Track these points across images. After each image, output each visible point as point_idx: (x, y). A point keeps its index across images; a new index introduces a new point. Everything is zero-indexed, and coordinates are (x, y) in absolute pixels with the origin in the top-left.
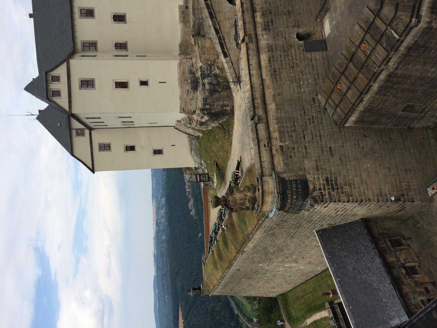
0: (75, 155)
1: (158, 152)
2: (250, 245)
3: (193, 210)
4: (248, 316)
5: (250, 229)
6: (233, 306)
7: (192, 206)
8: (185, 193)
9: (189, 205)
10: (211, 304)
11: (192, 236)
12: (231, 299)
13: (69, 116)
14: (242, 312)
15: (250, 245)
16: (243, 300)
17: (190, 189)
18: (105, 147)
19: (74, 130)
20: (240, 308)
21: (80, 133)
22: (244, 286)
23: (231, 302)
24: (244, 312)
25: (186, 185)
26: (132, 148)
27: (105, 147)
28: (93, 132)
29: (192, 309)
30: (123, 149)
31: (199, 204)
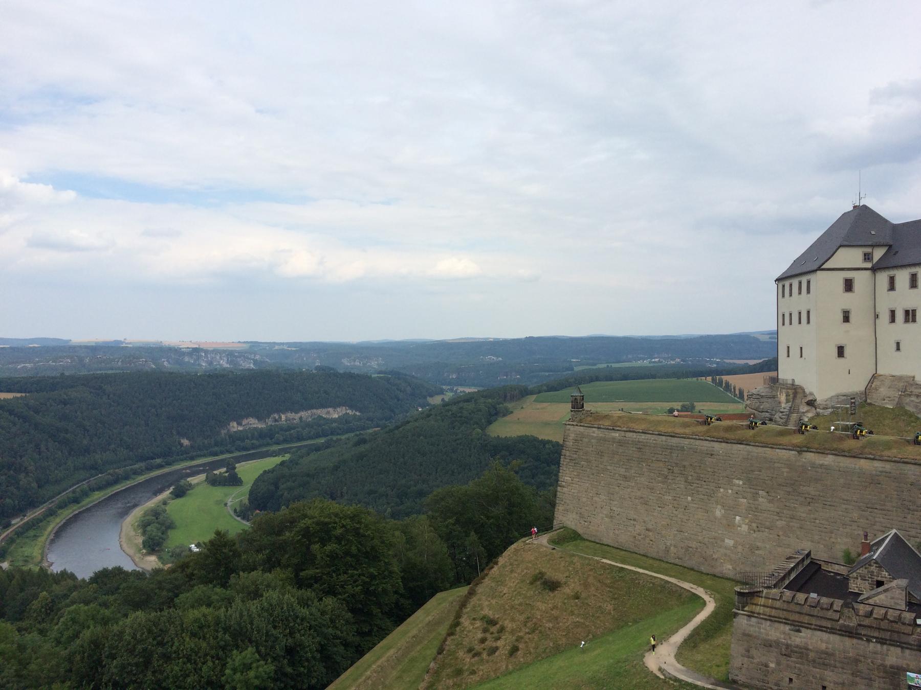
0: (841, 250)
1: (841, 351)
2: (827, 459)
3: (240, 428)
4: (10, 550)
5: (886, 453)
6: (28, 515)
7: (249, 426)
8: (279, 411)
9: (251, 419)
10: (32, 463)
11: (184, 423)
12: (46, 511)
13: (890, 246)
14: (18, 537)
15: (829, 460)
16: (47, 539)
17: (285, 423)
18: (849, 285)
19: (871, 251)
20: (27, 530)
21: (867, 257)
22: (624, 470)
23: (39, 509)
24: (18, 541)
25: (293, 414)
26: (846, 319)
27: (849, 285)
28: (868, 273)
29: (21, 420)
30: (846, 307)
31: (254, 442)
